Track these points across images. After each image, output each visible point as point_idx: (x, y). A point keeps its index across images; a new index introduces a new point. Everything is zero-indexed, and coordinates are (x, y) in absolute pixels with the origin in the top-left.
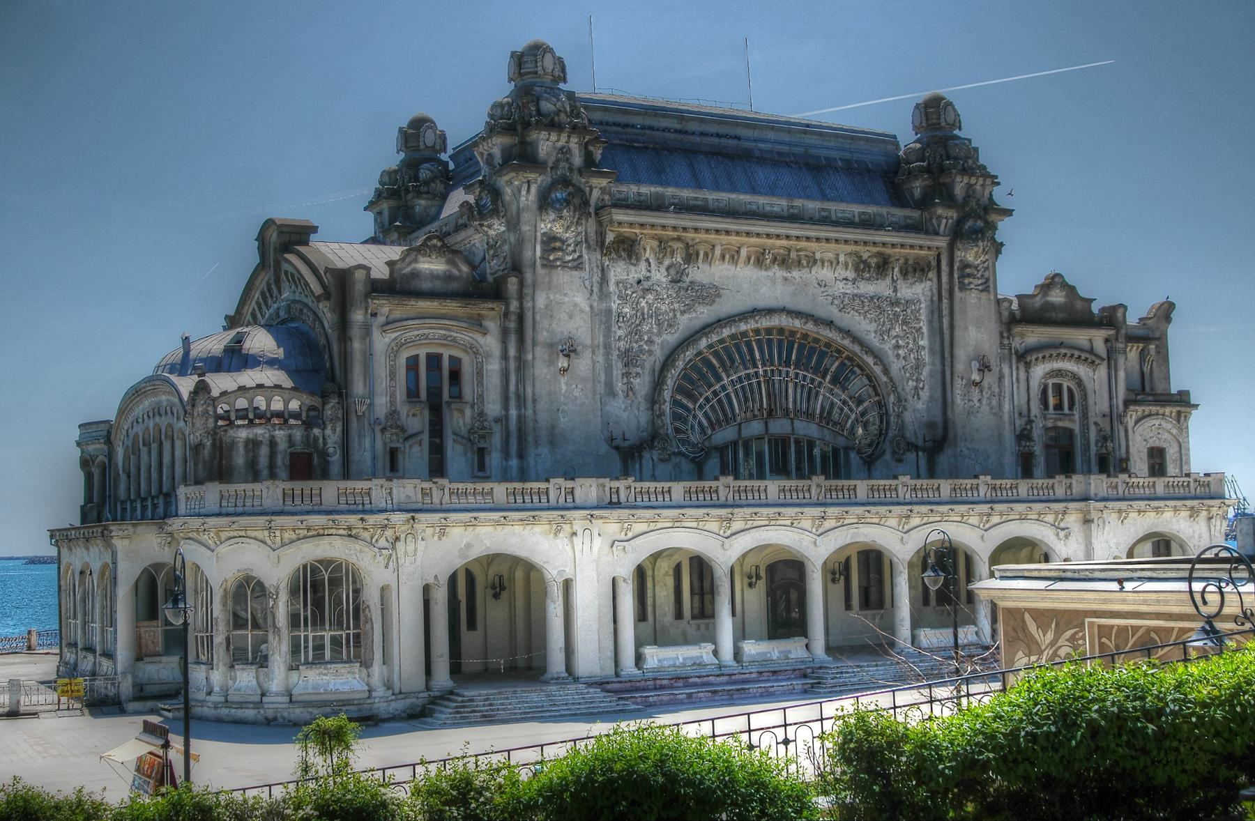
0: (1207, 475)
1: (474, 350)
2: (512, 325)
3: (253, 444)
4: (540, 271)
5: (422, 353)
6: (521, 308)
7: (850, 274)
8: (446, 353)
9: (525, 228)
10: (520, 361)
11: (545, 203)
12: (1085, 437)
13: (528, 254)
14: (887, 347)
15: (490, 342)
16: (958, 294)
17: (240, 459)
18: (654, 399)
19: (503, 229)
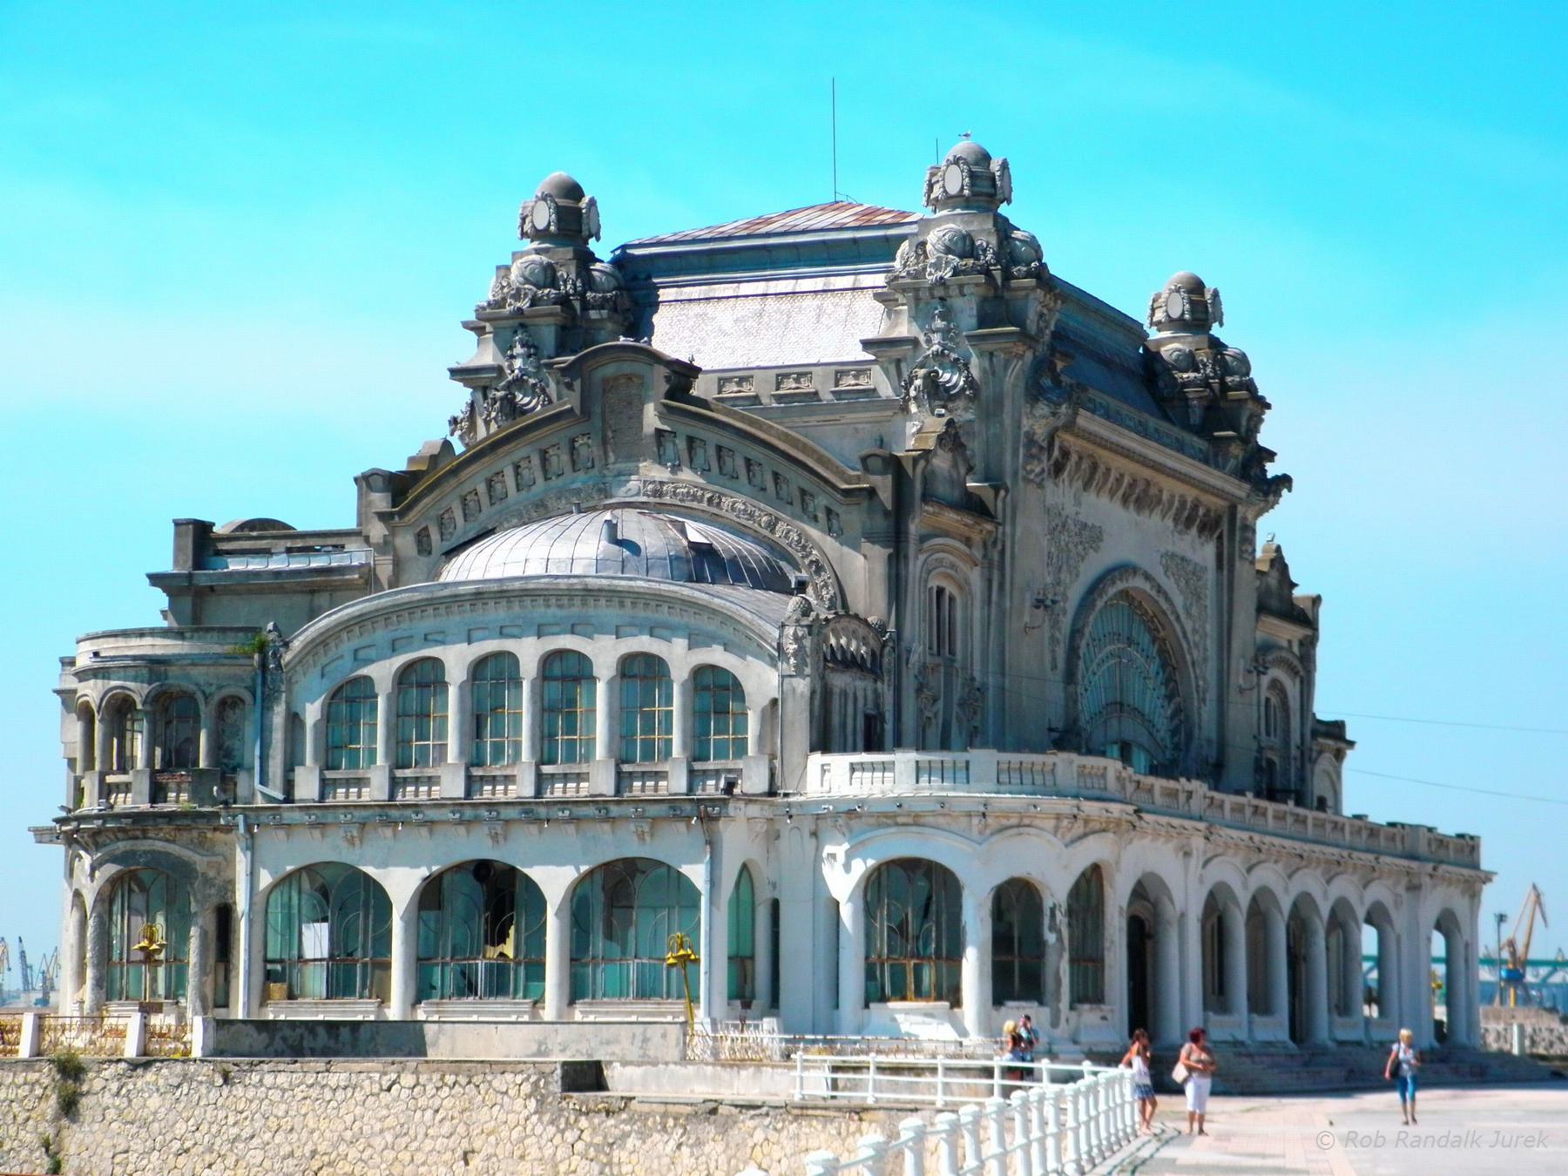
0: (1472, 838)
1: (963, 586)
2: (996, 557)
3: (844, 694)
4: (1021, 484)
5: (934, 583)
6: (1004, 533)
7: (1170, 523)
8: (950, 589)
9: (1007, 421)
10: (1000, 605)
11: (1035, 393)
12: (1286, 772)
13: (1008, 457)
14: (1188, 626)
15: (975, 577)
16: (1238, 564)
17: (836, 720)
18: (1070, 677)
19: (970, 416)
